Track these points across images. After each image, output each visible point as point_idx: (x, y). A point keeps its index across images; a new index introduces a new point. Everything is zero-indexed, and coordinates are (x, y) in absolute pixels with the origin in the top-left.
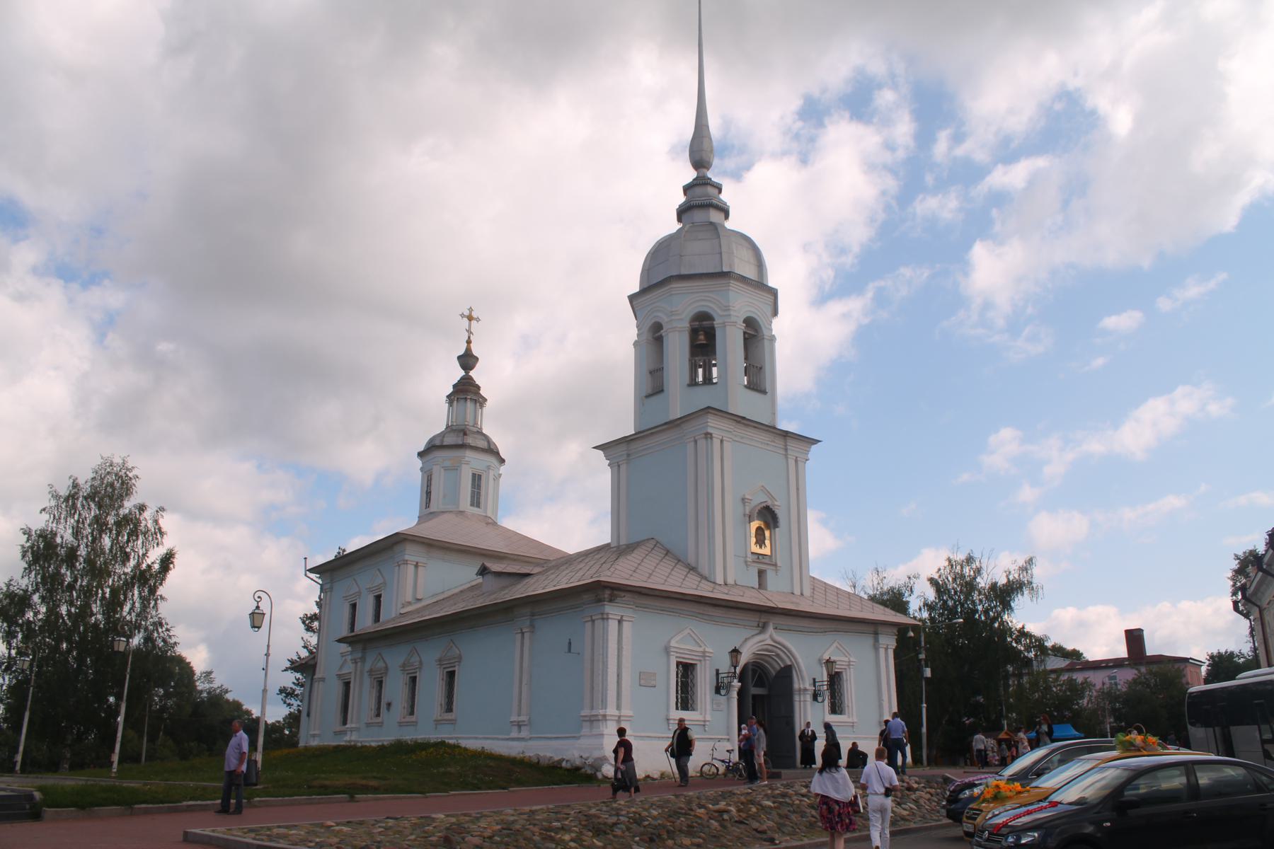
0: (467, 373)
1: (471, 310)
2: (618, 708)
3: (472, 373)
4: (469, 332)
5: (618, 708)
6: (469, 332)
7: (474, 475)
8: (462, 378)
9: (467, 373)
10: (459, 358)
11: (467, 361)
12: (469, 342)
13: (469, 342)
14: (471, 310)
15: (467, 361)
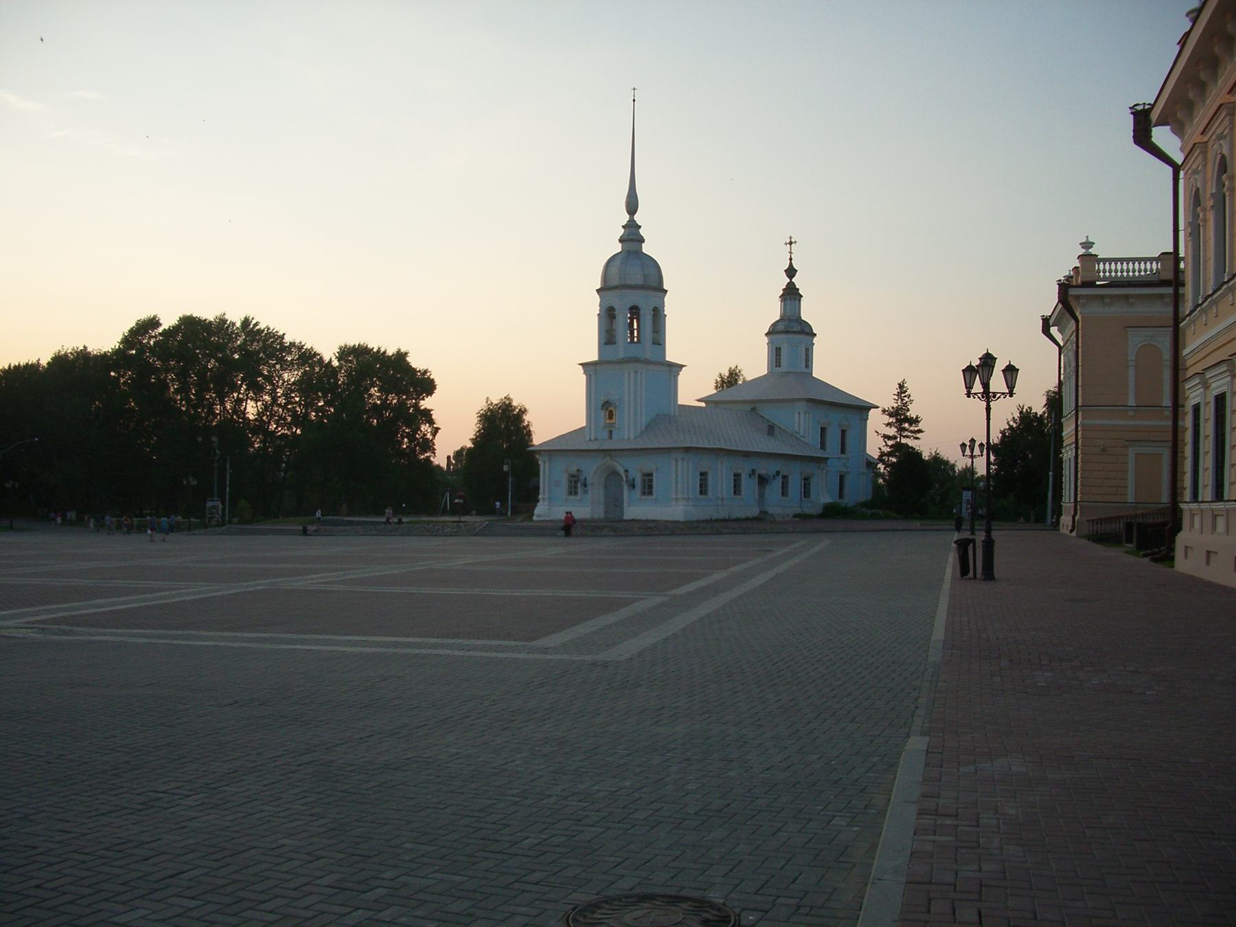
0: (791, 280)
1: (791, 238)
2: (544, 494)
3: (793, 280)
4: (791, 253)
5: (544, 494)
6: (791, 253)
7: (776, 348)
8: (788, 284)
9: (791, 280)
10: (785, 271)
11: (791, 272)
12: (791, 259)
13: (791, 259)
14: (791, 238)
15: (791, 272)
